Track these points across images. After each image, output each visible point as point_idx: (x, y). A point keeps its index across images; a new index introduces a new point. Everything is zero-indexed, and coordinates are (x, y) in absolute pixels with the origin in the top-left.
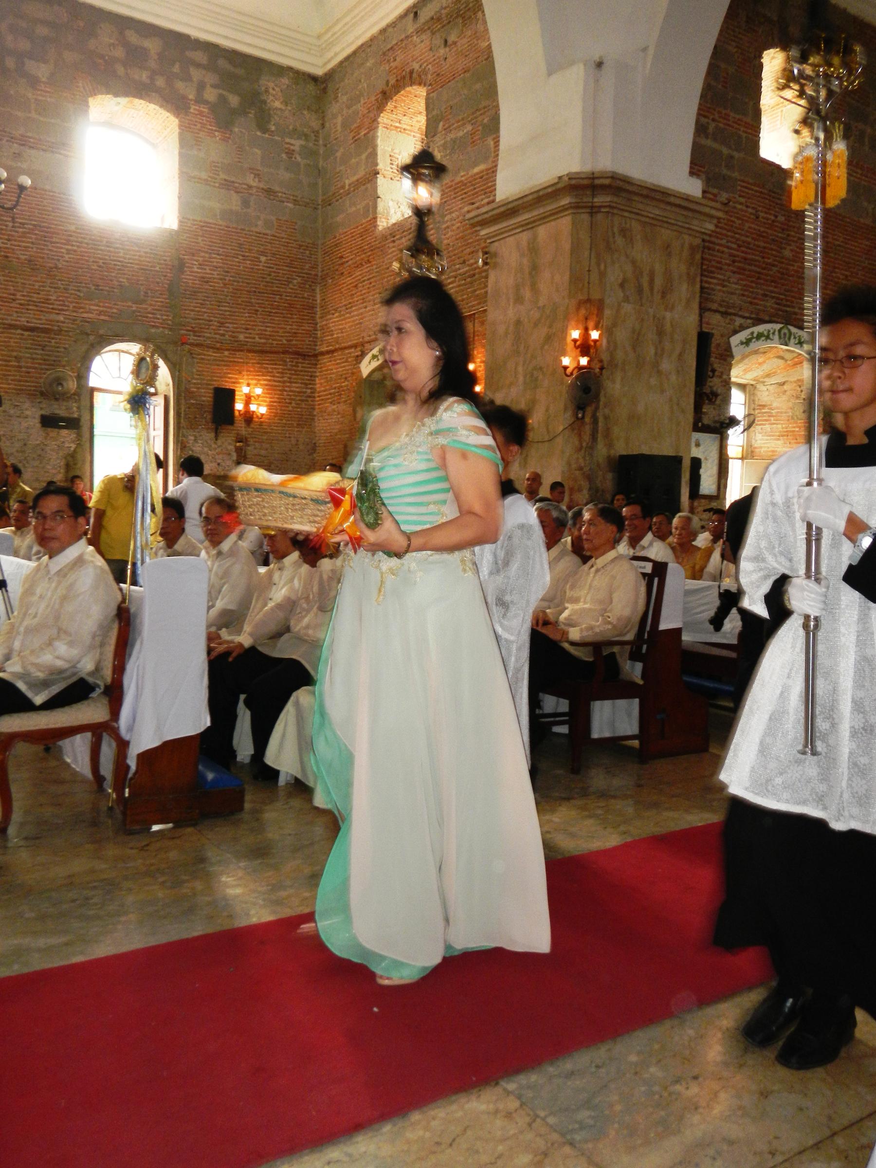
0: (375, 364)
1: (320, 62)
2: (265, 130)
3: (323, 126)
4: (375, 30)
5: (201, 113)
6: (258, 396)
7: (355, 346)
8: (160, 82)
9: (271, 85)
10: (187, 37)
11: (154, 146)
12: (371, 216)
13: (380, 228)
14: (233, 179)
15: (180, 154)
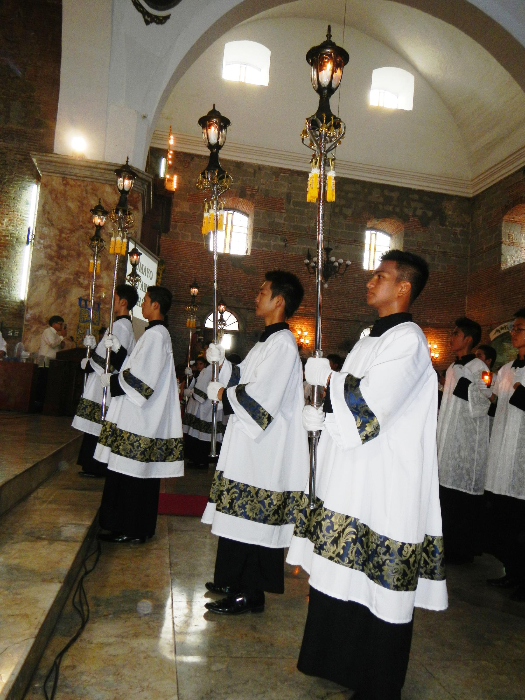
0: (497, 335)
1: (472, 191)
2: (443, 225)
3: (472, 220)
4: (502, 178)
5: (414, 221)
6: (435, 349)
7: (487, 325)
8: (398, 210)
9: (448, 204)
10: (410, 189)
11: (390, 235)
12: (497, 263)
13: (503, 269)
14: (428, 248)
15: (404, 239)
